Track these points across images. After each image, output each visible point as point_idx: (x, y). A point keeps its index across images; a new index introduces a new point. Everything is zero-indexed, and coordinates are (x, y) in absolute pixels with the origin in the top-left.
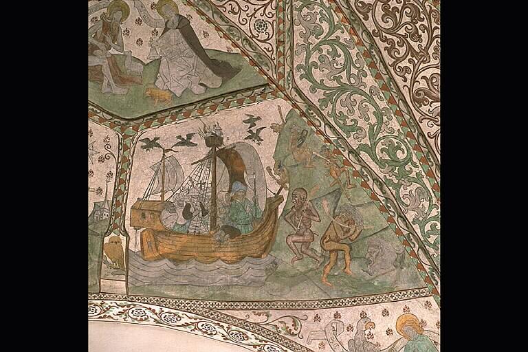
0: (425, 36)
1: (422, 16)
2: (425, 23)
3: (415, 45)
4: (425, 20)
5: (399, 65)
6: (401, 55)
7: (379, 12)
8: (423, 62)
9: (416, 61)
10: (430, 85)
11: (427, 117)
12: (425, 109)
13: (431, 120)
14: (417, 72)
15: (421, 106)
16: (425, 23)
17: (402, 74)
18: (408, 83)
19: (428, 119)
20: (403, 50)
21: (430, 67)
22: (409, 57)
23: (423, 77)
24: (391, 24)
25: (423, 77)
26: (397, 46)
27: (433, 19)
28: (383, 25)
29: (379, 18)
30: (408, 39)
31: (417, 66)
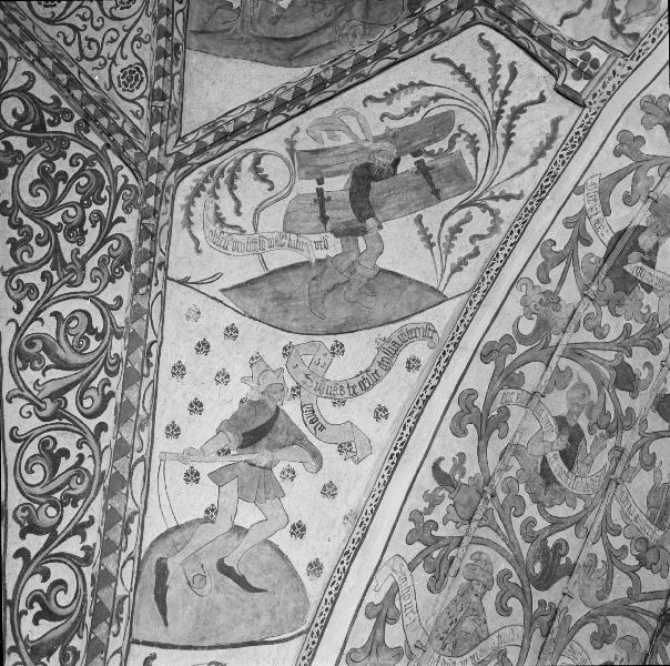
0: (93, 234)
1: (104, 193)
2: (104, 209)
3: (67, 248)
4: (107, 202)
5: (21, 277)
6: (34, 259)
7: (31, 173)
8: (70, 284)
9: (56, 279)
10: (62, 331)
11: (26, 393)
12: (29, 376)
13: (32, 403)
14: (48, 300)
15: (24, 368)
16: (104, 209)
17: (17, 296)
18: (21, 318)
19: (27, 399)
20: (40, 252)
21: (74, 296)
22: (47, 267)
23: (56, 314)
24: (42, 199)
25: (56, 314)
26: (33, 243)
27: (121, 201)
28: (26, 197)
29: (24, 185)
30: (61, 235)
31: (54, 288)
